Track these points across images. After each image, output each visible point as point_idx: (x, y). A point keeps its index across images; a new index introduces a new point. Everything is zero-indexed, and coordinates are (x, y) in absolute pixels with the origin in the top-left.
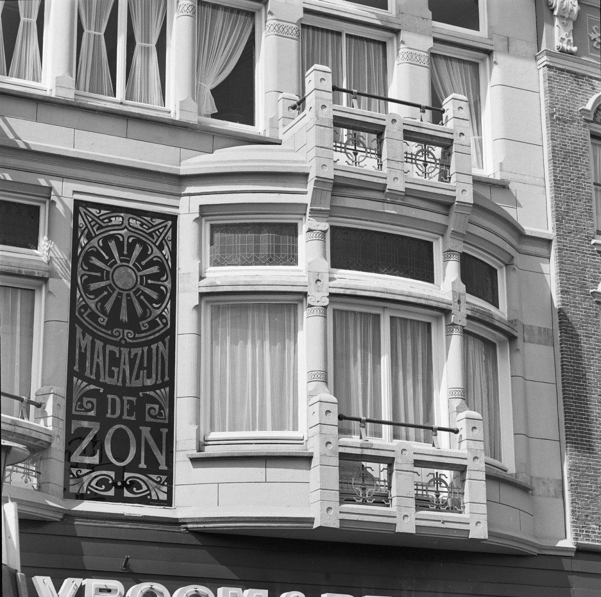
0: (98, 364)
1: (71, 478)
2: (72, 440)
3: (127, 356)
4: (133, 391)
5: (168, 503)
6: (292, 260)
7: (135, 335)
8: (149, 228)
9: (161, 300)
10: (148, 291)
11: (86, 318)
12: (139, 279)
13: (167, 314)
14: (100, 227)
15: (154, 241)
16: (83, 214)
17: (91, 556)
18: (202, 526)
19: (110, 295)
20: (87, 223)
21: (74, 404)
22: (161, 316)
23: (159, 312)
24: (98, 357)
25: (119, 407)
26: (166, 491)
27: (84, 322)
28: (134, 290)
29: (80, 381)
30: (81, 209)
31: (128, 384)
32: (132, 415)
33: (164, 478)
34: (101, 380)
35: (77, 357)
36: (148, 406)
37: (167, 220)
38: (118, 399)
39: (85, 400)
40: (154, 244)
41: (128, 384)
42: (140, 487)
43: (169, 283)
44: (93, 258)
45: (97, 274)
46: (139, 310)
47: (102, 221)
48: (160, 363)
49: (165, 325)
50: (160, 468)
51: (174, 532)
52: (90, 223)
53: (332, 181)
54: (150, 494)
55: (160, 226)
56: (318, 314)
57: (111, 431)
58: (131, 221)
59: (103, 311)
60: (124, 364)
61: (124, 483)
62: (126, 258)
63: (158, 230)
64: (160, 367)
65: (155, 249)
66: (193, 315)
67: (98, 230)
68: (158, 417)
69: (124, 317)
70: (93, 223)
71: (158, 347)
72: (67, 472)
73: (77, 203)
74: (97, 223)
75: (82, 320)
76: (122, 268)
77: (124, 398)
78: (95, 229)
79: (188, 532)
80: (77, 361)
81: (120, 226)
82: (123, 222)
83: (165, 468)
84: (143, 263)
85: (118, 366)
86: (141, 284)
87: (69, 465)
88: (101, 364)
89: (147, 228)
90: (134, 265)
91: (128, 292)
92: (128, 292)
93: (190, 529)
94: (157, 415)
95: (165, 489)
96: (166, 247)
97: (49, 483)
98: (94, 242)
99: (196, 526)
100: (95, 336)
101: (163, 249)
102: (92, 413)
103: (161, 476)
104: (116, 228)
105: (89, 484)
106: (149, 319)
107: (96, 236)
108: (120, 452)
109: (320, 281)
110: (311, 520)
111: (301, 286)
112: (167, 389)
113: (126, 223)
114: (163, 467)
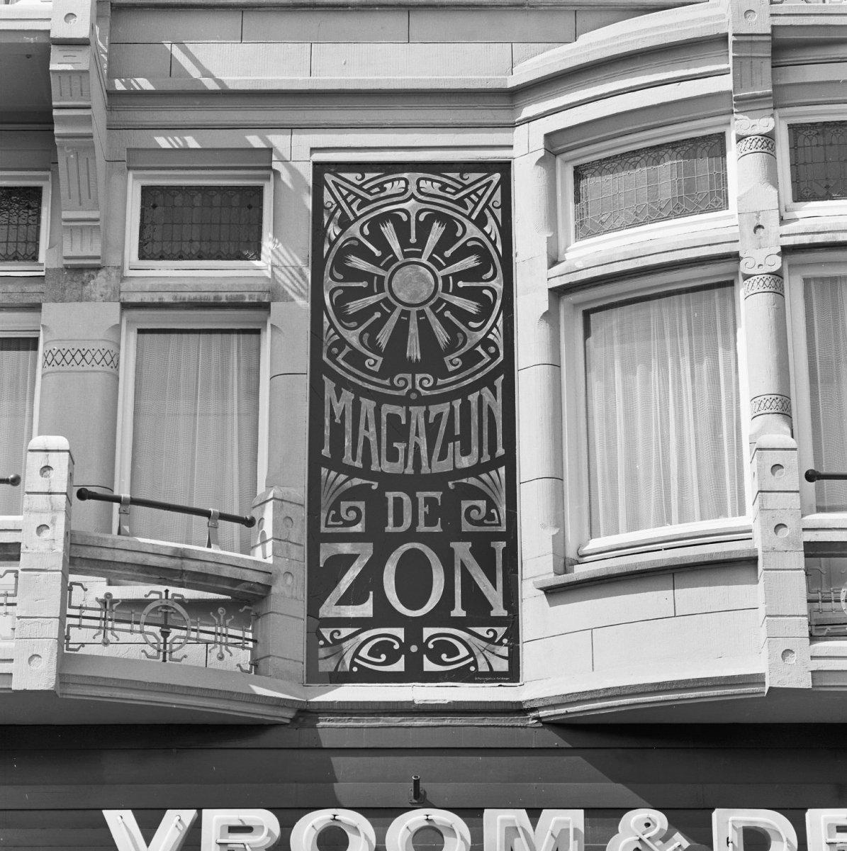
0: (366, 440)
1: (322, 646)
2: (321, 580)
3: (422, 420)
4: (436, 481)
5: (513, 675)
6: (717, 199)
7: (435, 381)
8: (458, 191)
9: (484, 314)
10: (458, 301)
11: (343, 363)
12: (440, 282)
13: (498, 337)
14: (365, 202)
15: (467, 213)
16: (332, 186)
18: (563, 711)
19: (385, 317)
20: (340, 198)
21: (323, 515)
22: (486, 343)
23: (480, 335)
24: (367, 428)
25: (409, 512)
26: (506, 654)
27: (339, 370)
28: (432, 302)
29: (333, 474)
30: (329, 178)
31: (425, 470)
32: (435, 524)
33: (501, 631)
34: (374, 468)
35: (327, 433)
36: (465, 505)
37: (491, 173)
38: (406, 498)
39: (344, 505)
40: (469, 217)
41: (425, 470)
42: (453, 651)
43: (499, 282)
44: (352, 258)
45: (360, 284)
46: (442, 336)
47: (368, 191)
48: (486, 425)
49: (494, 356)
50: (493, 613)
51: (513, 726)
52: (345, 198)
53: (769, 38)
54: (475, 663)
55: (479, 185)
56: (762, 290)
57: (396, 556)
58: (422, 183)
59: (374, 347)
60: (417, 434)
61: (423, 648)
62: (413, 251)
63: (474, 192)
64: (486, 433)
65: (470, 227)
66: (543, 330)
67: (359, 209)
68: (486, 521)
69: (414, 351)
70: (349, 199)
71: (480, 398)
72: (314, 635)
73: (319, 168)
74: (358, 196)
75: (335, 367)
76: (407, 269)
77: (418, 494)
78: (354, 207)
79: (541, 725)
80: (327, 440)
81: (404, 195)
82: (406, 189)
83: (505, 613)
84: (448, 254)
85: (405, 439)
86: (446, 289)
87: (316, 623)
88: (373, 439)
89: (453, 191)
90: (431, 259)
91: (420, 308)
92: (420, 308)
93: (544, 720)
94: (483, 520)
95: (504, 651)
96: (491, 221)
97: (269, 656)
98: (354, 230)
99: (552, 712)
100: (359, 392)
101: (486, 224)
102: (359, 528)
103: (495, 629)
104: (395, 199)
105: (356, 655)
106: (463, 351)
107: (357, 218)
109: (763, 228)
110: (757, 679)
111: (726, 242)
112: (502, 470)
113: (412, 188)
114: (499, 611)
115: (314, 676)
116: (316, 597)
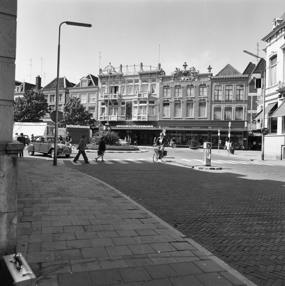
2: (126, 116)
17: (127, 123)
87: (126, 118)
108: (129, 117)
115: (126, 120)
116: (126, 117)
